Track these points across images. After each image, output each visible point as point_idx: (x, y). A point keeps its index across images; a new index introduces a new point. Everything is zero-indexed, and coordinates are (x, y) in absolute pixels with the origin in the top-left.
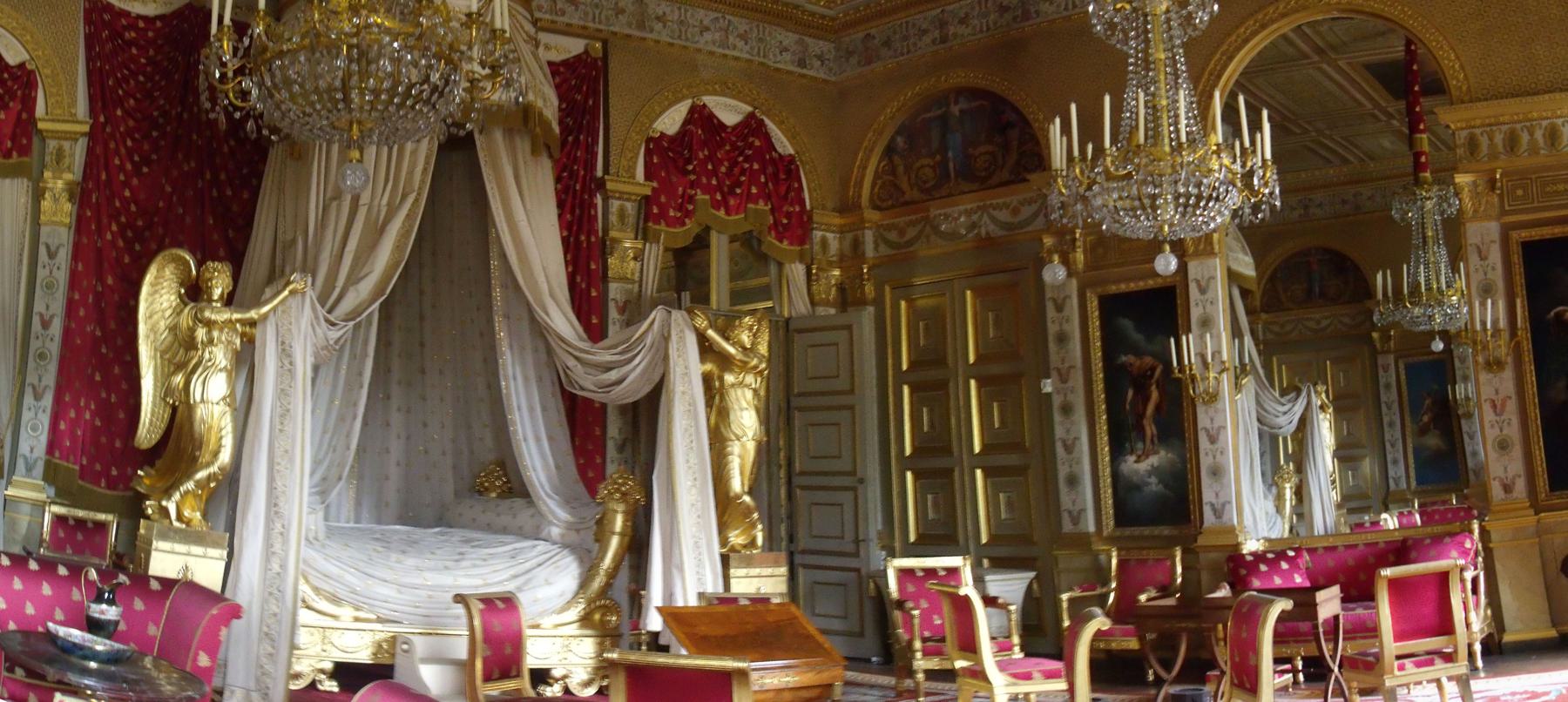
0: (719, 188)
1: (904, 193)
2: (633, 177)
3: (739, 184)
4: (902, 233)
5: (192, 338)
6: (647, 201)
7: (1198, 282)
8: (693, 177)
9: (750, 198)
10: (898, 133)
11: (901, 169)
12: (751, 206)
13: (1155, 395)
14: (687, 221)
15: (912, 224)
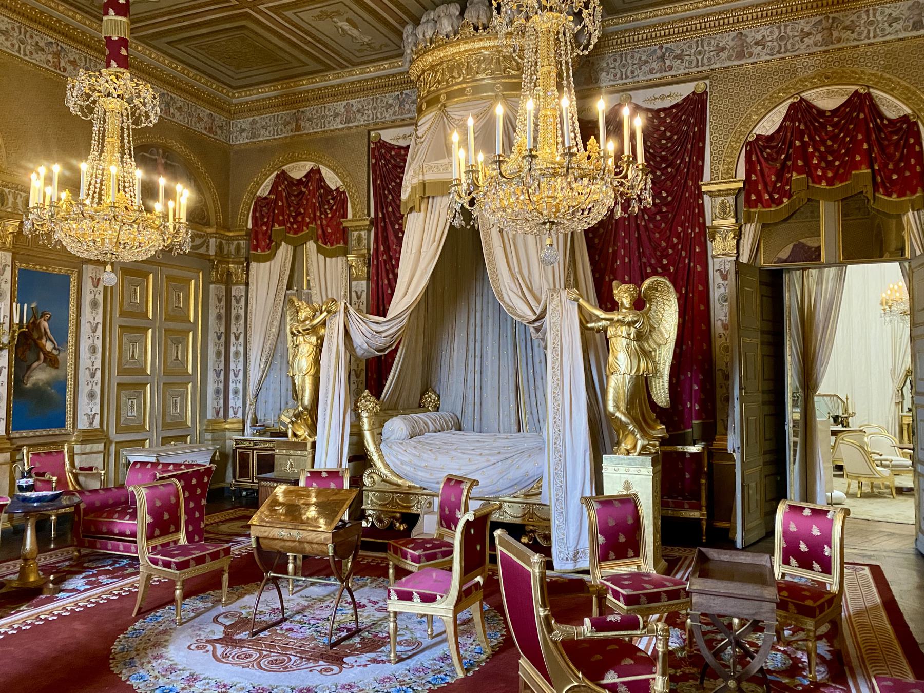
9: (857, 166)
14: (785, 200)
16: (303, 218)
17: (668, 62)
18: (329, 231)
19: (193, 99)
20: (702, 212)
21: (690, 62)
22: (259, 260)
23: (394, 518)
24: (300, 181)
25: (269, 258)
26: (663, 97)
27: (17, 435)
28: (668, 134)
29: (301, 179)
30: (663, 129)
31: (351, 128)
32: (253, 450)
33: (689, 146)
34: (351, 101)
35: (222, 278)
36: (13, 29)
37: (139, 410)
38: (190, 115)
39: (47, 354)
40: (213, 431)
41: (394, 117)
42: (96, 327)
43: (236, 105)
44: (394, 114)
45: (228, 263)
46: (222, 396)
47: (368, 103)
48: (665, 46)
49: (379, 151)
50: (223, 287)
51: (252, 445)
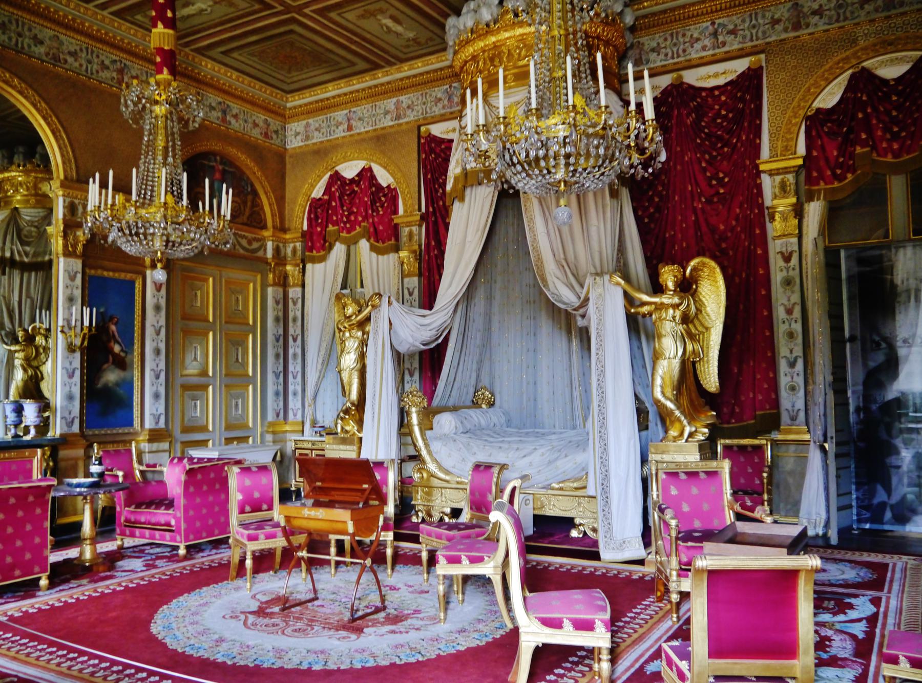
16: (356, 218)
17: (721, 38)
18: (381, 228)
19: (249, 106)
20: (760, 193)
21: (744, 37)
22: (314, 260)
23: (443, 513)
24: (352, 181)
25: (322, 259)
26: (716, 75)
27: (91, 433)
28: (724, 112)
29: (353, 178)
30: (717, 107)
31: (401, 124)
32: (312, 450)
33: (746, 124)
34: (401, 98)
35: (279, 280)
36: (81, 50)
37: (201, 411)
38: (246, 121)
39: (116, 356)
40: (274, 433)
41: (443, 111)
42: (160, 330)
43: (290, 109)
44: (444, 107)
45: (285, 265)
46: (281, 398)
47: (418, 99)
48: (717, 21)
49: (429, 146)
50: (281, 290)
51: (310, 446)
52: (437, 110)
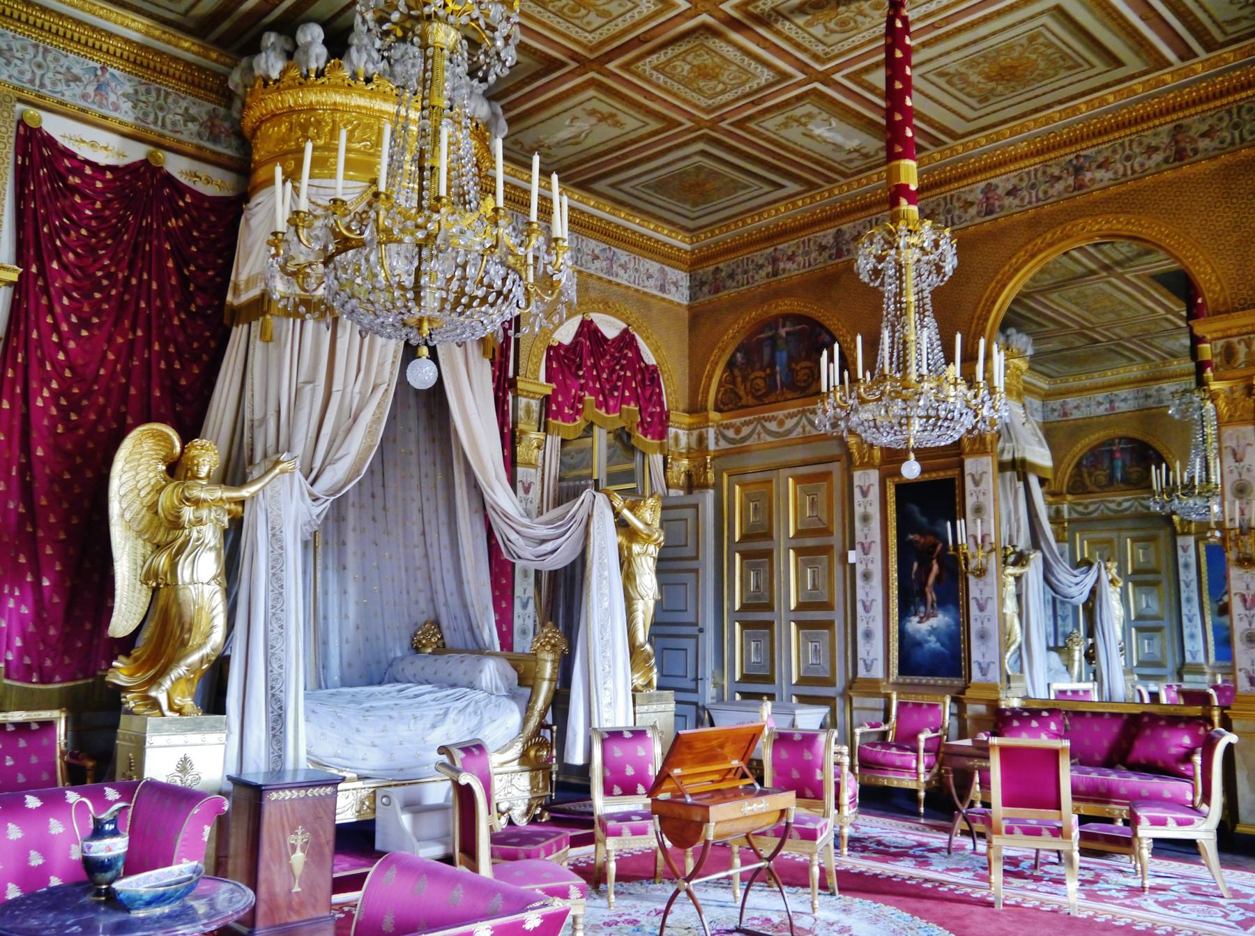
0: (602, 390)
1: (741, 399)
2: (537, 378)
3: (616, 388)
4: (738, 431)
5: (179, 517)
6: (547, 400)
7: (973, 476)
8: (582, 381)
9: (624, 400)
10: (737, 350)
11: (739, 379)
12: (624, 406)
13: (935, 568)
15: (747, 423)
41: (82, 104)
44: (85, 97)
52: (67, 93)
